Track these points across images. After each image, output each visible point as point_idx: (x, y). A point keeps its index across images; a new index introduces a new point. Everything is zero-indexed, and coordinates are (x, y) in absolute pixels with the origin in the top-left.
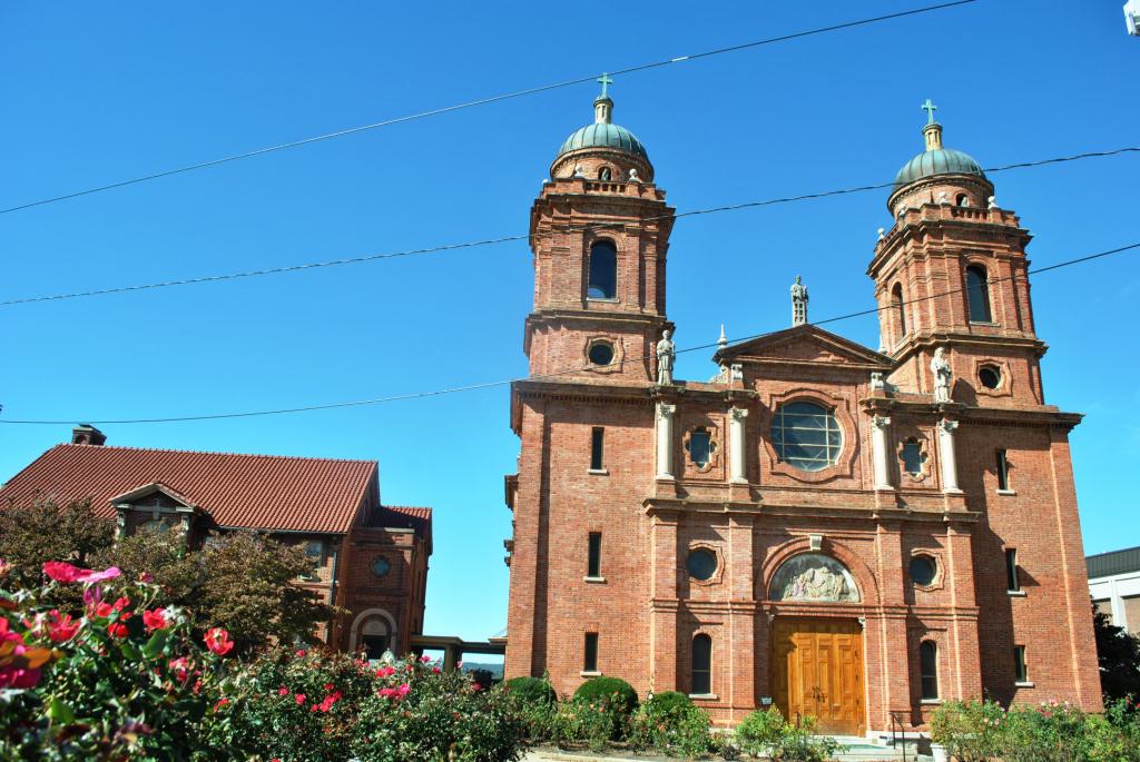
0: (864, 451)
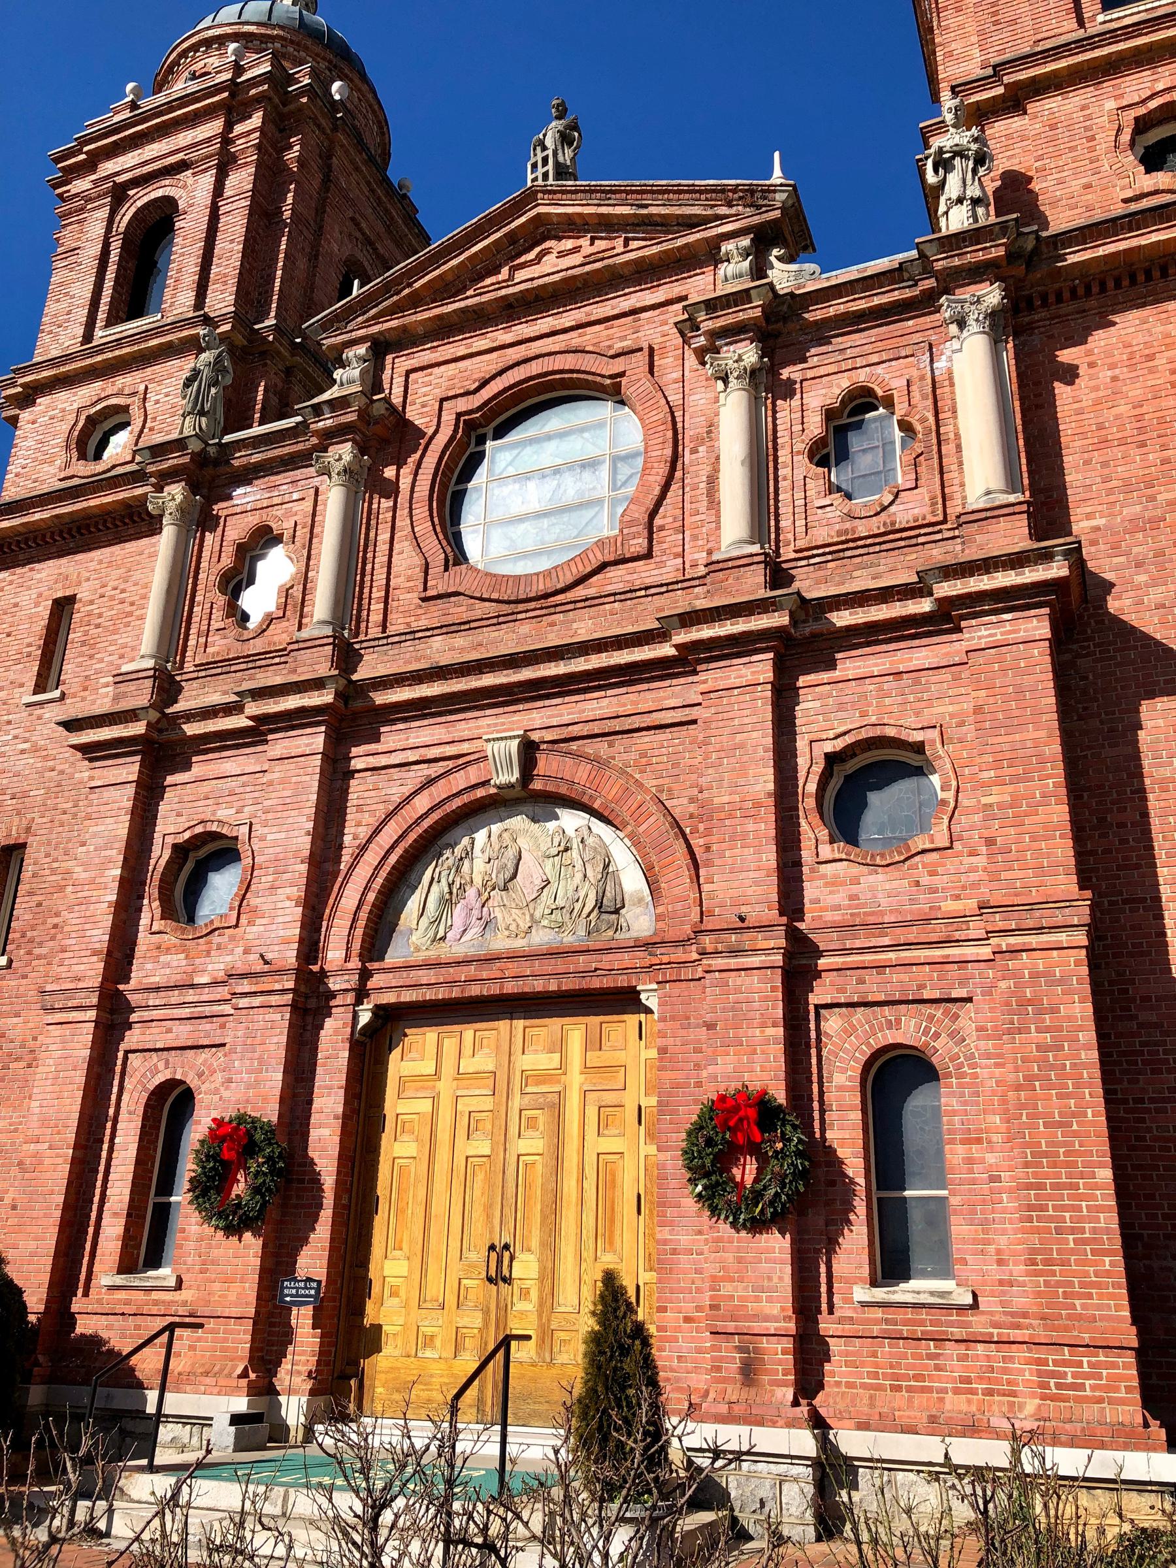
0: (695, 461)
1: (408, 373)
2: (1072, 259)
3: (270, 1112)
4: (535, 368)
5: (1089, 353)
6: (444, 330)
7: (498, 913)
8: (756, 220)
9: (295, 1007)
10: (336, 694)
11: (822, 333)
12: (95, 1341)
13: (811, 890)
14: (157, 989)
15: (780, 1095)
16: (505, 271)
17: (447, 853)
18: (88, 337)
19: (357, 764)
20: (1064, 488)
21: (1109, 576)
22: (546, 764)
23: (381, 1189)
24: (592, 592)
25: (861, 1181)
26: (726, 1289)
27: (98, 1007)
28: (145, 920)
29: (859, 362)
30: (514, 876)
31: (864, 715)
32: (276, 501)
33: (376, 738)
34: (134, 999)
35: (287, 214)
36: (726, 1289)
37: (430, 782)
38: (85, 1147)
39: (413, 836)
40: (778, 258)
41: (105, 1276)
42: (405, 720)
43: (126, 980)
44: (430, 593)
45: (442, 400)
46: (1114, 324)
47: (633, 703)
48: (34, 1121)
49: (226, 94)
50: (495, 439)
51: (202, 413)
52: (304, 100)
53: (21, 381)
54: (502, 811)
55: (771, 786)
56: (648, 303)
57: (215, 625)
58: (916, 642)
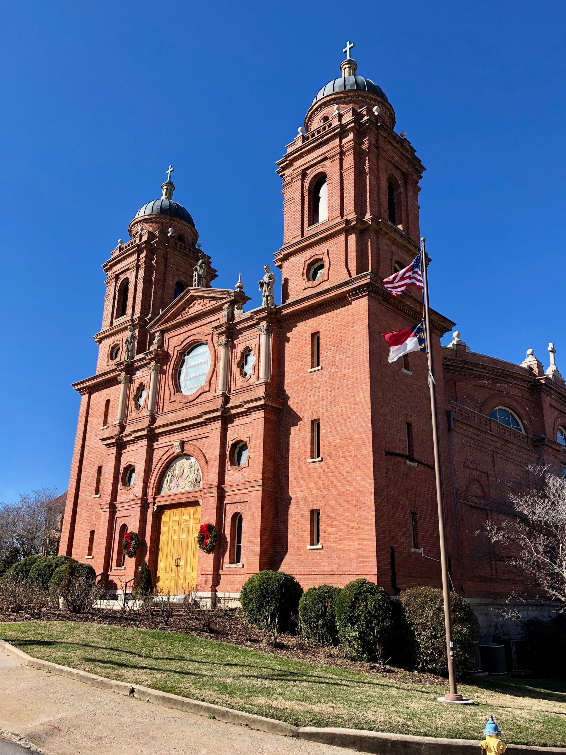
1: (169, 339)
2: (284, 313)
3: (137, 531)
4: (191, 338)
5: (292, 334)
6: (175, 327)
7: (180, 483)
8: (229, 300)
9: (141, 507)
10: (147, 431)
11: (241, 331)
12: (112, 581)
13: (227, 477)
14: (120, 503)
15: (214, 524)
16: (187, 309)
17: (172, 468)
18: (111, 324)
19: (155, 447)
20: (284, 372)
21: (289, 395)
22: (186, 447)
23: (160, 547)
24: (204, 399)
25: (229, 542)
26: (204, 565)
27: (110, 508)
28: (119, 487)
29: (247, 339)
30: (183, 474)
31: (238, 434)
32: (144, 375)
33: (157, 441)
34: (117, 505)
35: (154, 280)
36: (204, 565)
37: (166, 452)
38: (109, 540)
39: (164, 465)
40: (237, 308)
41: (114, 568)
42: (163, 436)
43: (116, 501)
44: (171, 401)
45: (174, 347)
46: (297, 326)
47: (201, 431)
48: (100, 534)
49: (136, 248)
50: (188, 355)
51: (129, 351)
52: (155, 245)
53: (98, 338)
54: (181, 458)
55: (219, 453)
56: (213, 320)
57: (133, 410)
58: (247, 416)
